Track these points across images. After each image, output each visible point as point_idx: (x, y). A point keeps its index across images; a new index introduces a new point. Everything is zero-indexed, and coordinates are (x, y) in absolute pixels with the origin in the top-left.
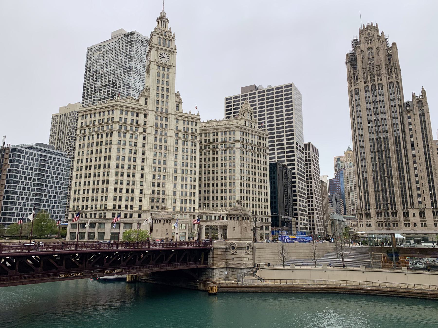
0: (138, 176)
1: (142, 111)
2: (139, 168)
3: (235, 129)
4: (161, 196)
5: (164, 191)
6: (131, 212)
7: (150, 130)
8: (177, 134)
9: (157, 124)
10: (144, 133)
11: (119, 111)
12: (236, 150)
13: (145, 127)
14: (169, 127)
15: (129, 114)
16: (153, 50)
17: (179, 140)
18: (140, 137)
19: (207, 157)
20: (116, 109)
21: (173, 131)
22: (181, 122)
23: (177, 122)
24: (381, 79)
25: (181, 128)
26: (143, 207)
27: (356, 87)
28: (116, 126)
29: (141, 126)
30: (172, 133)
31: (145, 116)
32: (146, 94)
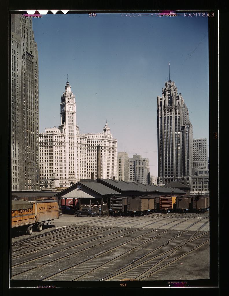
0: (64, 165)
2: (63, 161)
4: (73, 174)
5: (73, 171)
7: (67, 144)
9: (69, 141)
11: (55, 137)
13: (65, 143)
14: (74, 142)
15: (59, 137)
18: (63, 148)
19: (89, 153)
22: (79, 139)
23: (78, 140)
25: (79, 142)
28: (54, 144)
29: (64, 143)
30: (75, 145)
31: (65, 137)
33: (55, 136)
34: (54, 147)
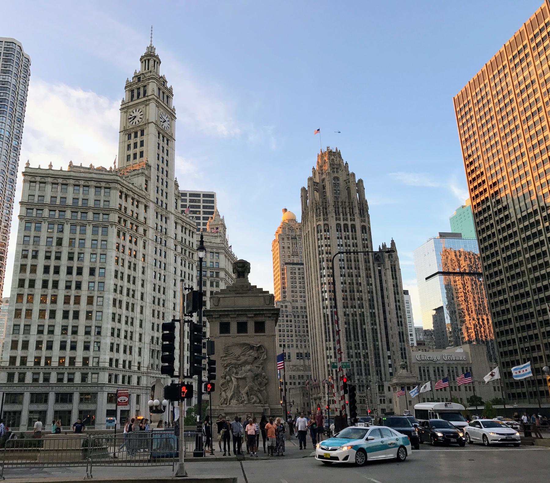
1: (143, 201)
2: (138, 295)
3: (220, 251)
6: (131, 374)
7: (151, 234)
8: (176, 246)
10: (144, 238)
12: (220, 282)
15: (130, 200)
16: (153, 105)
17: (177, 257)
20: (116, 188)
21: (172, 241)
23: (176, 228)
24: (354, 220)
25: (179, 239)
26: (142, 365)
27: (326, 222)
30: (171, 243)
32: (146, 172)
33: (121, 192)
34: (113, 231)
